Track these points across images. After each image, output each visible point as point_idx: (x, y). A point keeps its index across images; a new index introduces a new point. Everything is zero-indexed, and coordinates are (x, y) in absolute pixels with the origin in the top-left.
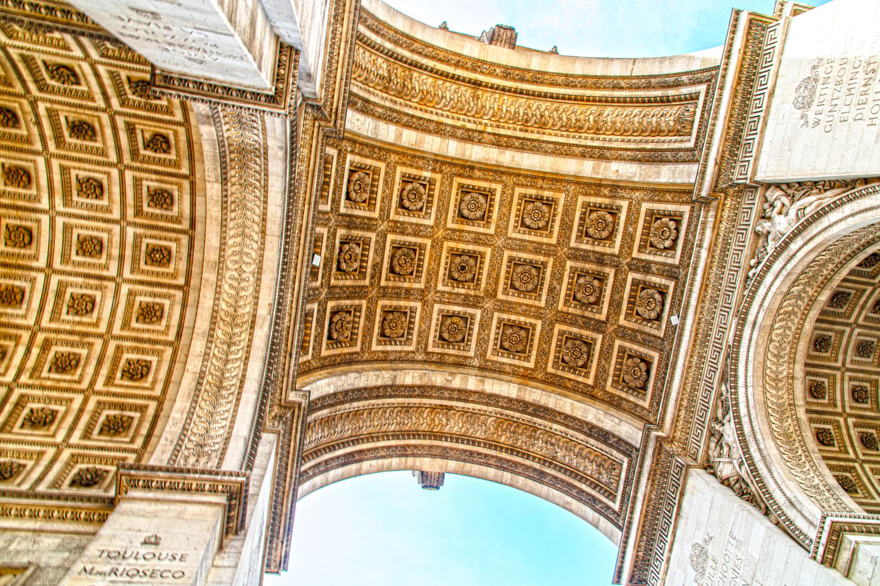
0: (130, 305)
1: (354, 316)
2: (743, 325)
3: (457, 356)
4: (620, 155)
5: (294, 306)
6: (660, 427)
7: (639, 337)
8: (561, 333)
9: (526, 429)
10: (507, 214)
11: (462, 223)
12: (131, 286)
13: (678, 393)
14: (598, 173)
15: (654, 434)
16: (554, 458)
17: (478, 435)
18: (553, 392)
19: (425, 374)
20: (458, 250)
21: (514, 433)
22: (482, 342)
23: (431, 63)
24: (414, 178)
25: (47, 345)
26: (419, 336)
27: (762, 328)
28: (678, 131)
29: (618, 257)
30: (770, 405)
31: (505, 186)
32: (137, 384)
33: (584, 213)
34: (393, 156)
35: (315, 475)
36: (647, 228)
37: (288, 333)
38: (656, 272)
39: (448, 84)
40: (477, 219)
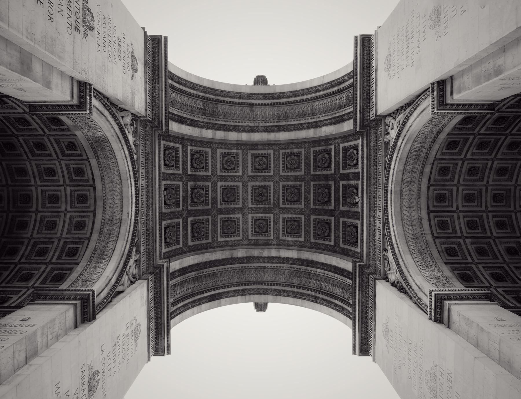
0: (70, 222)
1: (206, 225)
2: (387, 193)
4: (325, 123)
5: (154, 217)
6: (361, 260)
7: (350, 214)
8: (315, 220)
9: (305, 274)
10: (278, 164)
11: (256, 172)
12: (71, 214)
14: (317, 135)
15: (358, 264)
16: (321, 288)
17: (281, 280)
18: (315, 252)
20: (256, 186)
21: (299, 277)
23: (226, 99)
24: (228, 154)
25: (35, 244)
26: (243, 232)
27: (395, 192)
28: (348, 104)
29: (334, 174)
30: (409, 235)
31: (275, 151)
32: (72, 258)
34: (214, 145)
35: (193, 307)
36: (345, 156)
37: (153, 230)
39: (237, 107)
40: (264, 169)
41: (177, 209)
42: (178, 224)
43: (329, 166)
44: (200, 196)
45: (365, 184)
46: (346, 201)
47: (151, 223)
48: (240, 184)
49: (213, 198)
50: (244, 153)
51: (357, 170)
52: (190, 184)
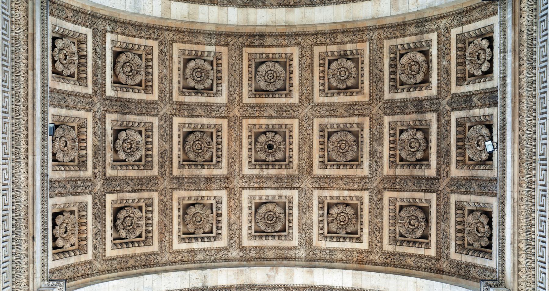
1: (147, 211)
3: (279, 249)
7: (474, 185)
8: (392, 202)
10: (310, 78)
11: (261, 96)
13: (513, 234)
14: (397, 10)
19: (242, 272)
20: (260, 126)
22: (305, 228)
26: (230, 229)
31: (302, 48)
33: (395, 59)
34: (166, 33)
36: (461, 56)
37: (27, 213)
38: (479, 103)
41: (82, 174)
42: (83, 208)
43: (426, 81)
44: (131, 149)
45: (509, 110)
46: (463, 155)
47: (23, 197)
48: (224, 123)
49: (162, 153)
50: (232, 52)
51: (489, 85)
52: (110, 118)
